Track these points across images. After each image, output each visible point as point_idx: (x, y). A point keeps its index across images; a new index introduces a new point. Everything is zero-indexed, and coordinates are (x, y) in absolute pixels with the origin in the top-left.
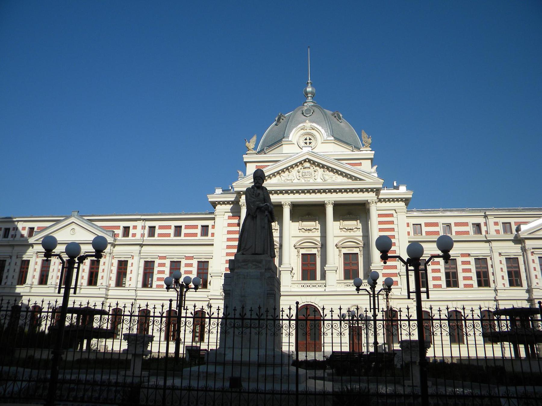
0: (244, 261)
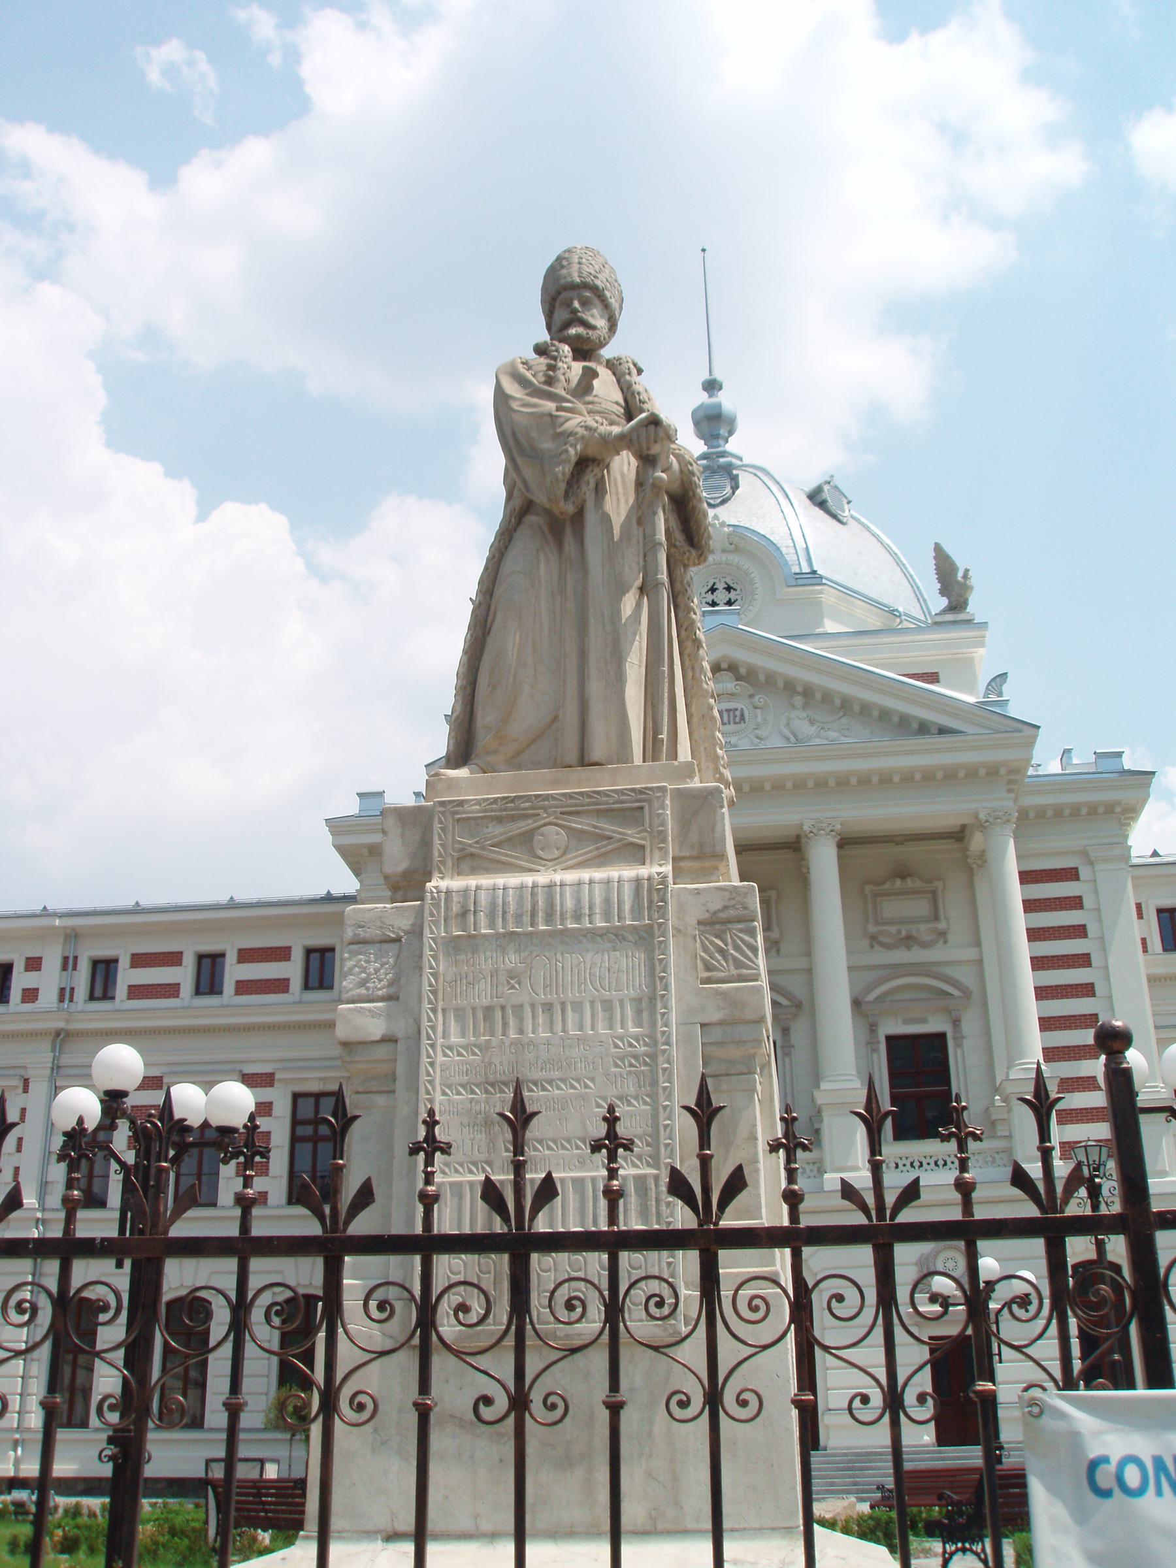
0: (508, 811)
